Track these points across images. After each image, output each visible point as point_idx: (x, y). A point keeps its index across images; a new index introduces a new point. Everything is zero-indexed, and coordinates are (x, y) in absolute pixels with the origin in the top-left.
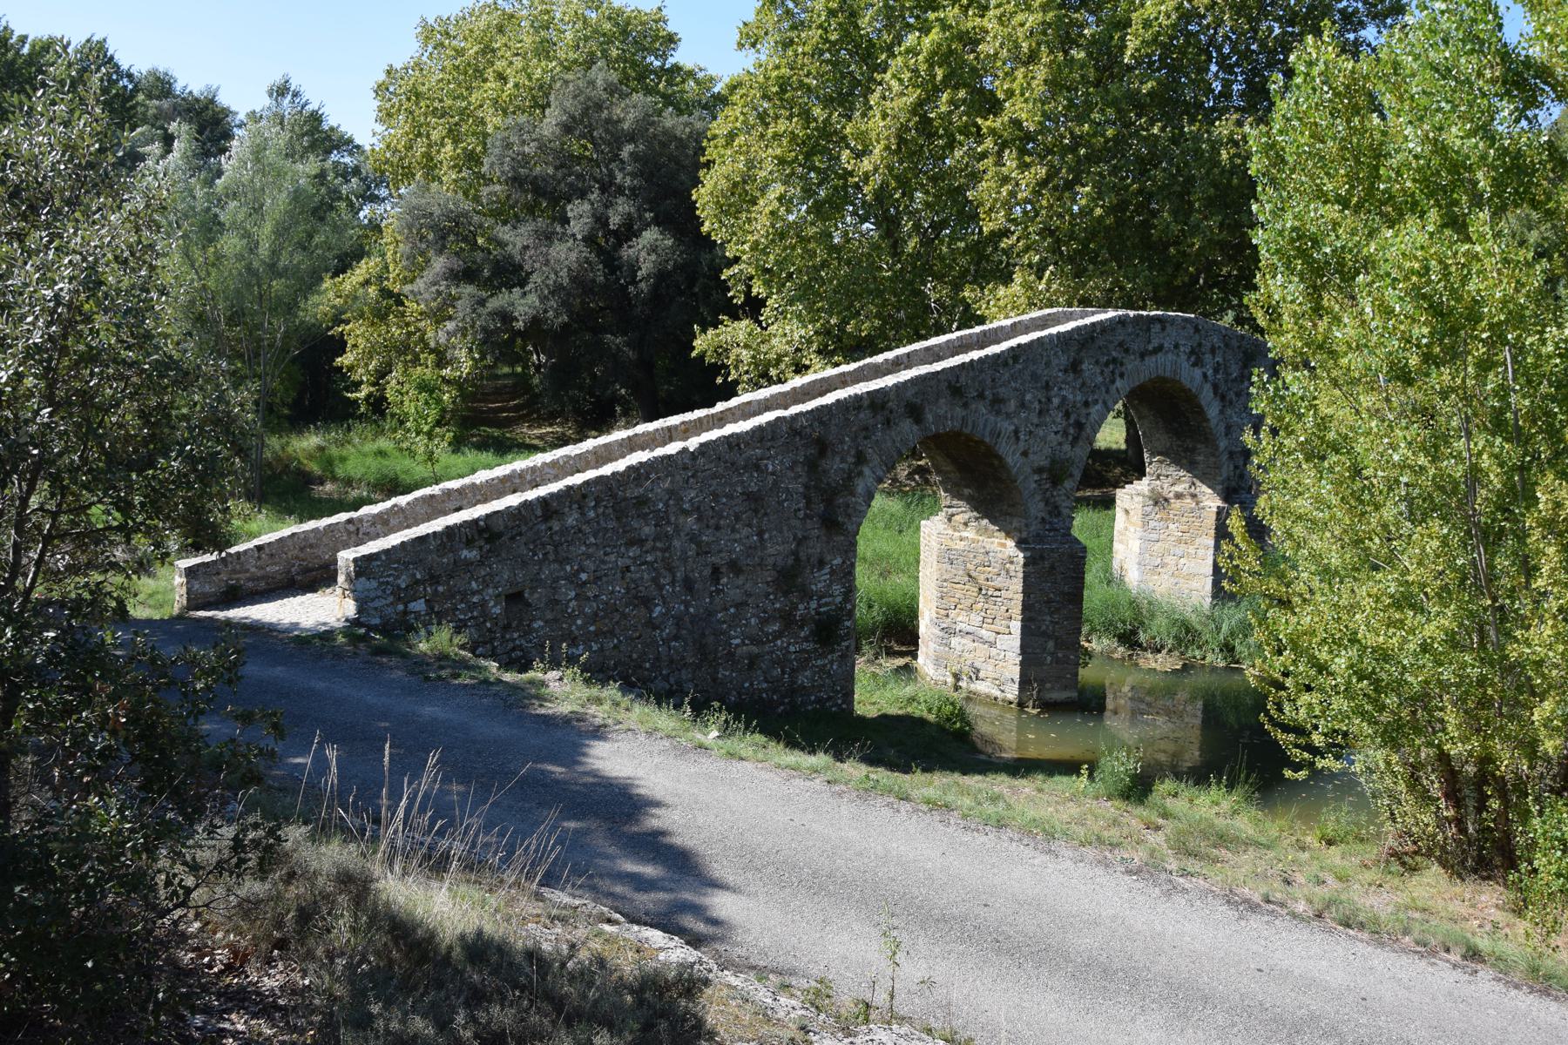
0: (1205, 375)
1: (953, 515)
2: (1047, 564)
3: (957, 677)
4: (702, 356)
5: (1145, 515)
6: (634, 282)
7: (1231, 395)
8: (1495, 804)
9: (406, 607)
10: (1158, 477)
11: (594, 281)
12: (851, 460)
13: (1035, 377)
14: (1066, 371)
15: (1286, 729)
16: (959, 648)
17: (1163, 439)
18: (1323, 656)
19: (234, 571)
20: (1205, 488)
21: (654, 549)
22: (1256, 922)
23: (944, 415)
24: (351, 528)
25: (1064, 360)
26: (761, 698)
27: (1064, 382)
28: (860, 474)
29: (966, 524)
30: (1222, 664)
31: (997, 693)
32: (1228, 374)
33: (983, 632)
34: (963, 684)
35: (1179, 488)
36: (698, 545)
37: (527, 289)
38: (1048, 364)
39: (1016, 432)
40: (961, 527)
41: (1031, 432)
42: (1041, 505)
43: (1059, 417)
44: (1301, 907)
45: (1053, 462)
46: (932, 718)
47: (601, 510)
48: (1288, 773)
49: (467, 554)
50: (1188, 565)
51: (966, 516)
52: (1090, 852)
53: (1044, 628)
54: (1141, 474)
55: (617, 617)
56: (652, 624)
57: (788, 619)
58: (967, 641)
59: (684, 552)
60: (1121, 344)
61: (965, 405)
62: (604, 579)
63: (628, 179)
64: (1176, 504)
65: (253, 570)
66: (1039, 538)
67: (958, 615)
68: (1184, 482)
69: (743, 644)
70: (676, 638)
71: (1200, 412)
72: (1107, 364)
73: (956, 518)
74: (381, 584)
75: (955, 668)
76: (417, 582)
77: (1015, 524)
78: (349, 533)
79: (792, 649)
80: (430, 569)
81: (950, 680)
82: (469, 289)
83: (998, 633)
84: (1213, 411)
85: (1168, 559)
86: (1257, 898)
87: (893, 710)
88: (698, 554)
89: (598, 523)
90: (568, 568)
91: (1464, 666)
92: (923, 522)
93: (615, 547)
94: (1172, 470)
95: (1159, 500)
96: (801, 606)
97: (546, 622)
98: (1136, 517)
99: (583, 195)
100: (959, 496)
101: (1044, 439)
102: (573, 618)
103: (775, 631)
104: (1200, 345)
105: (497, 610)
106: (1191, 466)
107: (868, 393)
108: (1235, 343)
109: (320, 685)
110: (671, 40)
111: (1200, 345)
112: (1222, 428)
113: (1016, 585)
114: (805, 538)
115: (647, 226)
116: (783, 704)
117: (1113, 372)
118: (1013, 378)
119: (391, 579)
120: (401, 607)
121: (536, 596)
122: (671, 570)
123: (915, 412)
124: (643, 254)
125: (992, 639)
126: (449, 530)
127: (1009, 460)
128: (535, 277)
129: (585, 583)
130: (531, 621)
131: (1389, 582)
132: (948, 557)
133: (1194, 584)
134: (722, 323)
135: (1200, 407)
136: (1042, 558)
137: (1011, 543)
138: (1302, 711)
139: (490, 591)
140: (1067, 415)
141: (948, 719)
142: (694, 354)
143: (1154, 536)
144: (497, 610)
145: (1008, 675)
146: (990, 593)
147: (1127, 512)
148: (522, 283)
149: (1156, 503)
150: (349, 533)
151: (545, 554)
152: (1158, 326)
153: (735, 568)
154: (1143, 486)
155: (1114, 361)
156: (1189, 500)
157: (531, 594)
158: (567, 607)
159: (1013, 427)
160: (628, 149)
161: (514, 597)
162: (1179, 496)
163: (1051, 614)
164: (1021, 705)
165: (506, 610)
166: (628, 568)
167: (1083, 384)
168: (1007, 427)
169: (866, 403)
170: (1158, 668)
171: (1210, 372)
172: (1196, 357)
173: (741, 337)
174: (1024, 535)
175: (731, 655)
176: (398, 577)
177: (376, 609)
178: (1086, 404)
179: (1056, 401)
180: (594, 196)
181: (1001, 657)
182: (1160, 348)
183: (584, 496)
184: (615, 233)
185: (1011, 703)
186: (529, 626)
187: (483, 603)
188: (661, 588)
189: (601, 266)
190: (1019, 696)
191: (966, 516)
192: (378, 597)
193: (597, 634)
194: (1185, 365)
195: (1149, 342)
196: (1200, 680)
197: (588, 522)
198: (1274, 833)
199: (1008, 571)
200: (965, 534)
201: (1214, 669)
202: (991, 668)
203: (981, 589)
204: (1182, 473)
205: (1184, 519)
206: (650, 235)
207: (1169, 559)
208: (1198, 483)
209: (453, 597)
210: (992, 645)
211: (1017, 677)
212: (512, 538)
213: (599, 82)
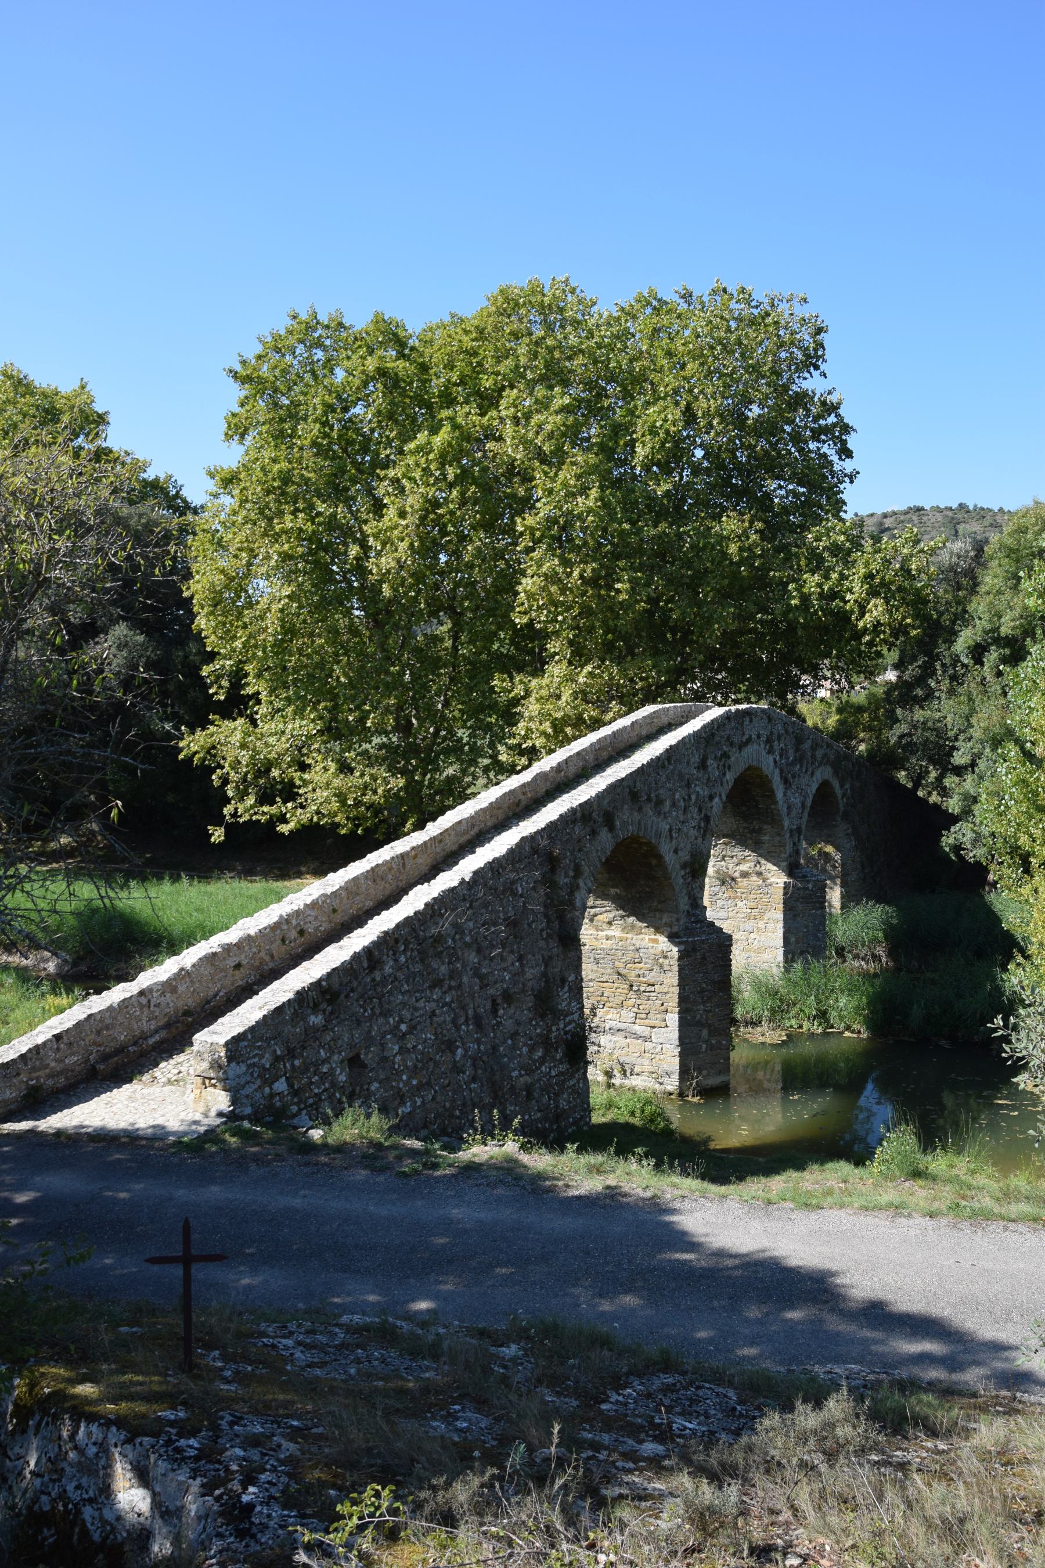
0: (775, 762)
1: (596, 915)
2: (699, 955)
4: (189, 759)
9: (271, 1089)
10: (724, 857)
12: (571, 874)
13: (681, 776)
14: (698, 768)
16: (610, 1046)
19: (34, 1069)
20: (770, 866)
21: (450, 988)
25: (696, 759)
26: (537, 1127)
28: (578, 887)
29: (610, 923)
30: (820, 1031)
33: (637, 1028)
34: (617, 1081)
35: (744, 867)
36: (481, 977)
38: (688, 763)
39: (670, 830)
40: (605, 926)
41: (679, 830)
42: (686, 898)
46: (637, 1121)
47: (409, 954)
50: (758, 939)
51: (611, 915)
53: (698, 1017)
55: (431, 1065)
56: (457, 1069)
57: (546, 1042)
58: (618, 1038)
59: (471, 987)
61: (640, 809)
62: (419, 1027)
64: (743, 882)
65: (53, 1064)
66: (689, 931)
67: (607, 1013)
68: (748, 861)
69: (521, 1075)
70: (474, 1079)
71: (771, 795)
73: (599, 917)
74: (249, 1066)
75: (607, 1066)
77: (665, 919)
78: (142, 1006)
79: (553, 1073)
80: (287, 1043)
83: (654, 1027)
84: (779, 795)
88: (481, 988)
89: (407, 967)
90: (391, 1020)
93: (422, 991)
94: (738, 852)
96: (554, 1028)
97: (380, 1083)
100: (604, 896)
102: (399, 1073)
103: (540, 1058)
107: (580, 805)
109: (297, 1202)
112: (785, 809)
113: (671, 981)
114: (551, 958)
115: (114, 621)
116: (552, 1131)
117: (724, 765)
119: (256, 1060)
120: (267, 1090)
121: (370, 1055)
122: (464, 1008)
125: (647, 1034)
126: (301, 995)
127: (667, 859)
129: (404, 1035)
130: (369, 1084)
134: (212, 723)
136: (694, 950)
137: (663, 939)
139: (336, 1057)
140: (700, 810)
141: (652, 1121)
142: (181, 757)
144: (343, 1078)
145: (666, 1067)
146: (642, 989)
149: (723, 883)
150: (142, 1006)
151: (372, 1009)
152: (748, 719)
153: (508, 997)
156: (755, 878)
157: (366, 1054)
158: (394, 1063)
159: (668, 827)
161: (354, 1062)
162: (745, 875)
163: (704, 1003)
164: (681, 1095)
165: (350, 1076)
166: (433, 1014)
167: (708, 779)
169: (579, 814)
170: (768, 1041)
171: (778, 758)
173: (238, 736)
174: (675, 929)
175: (513, 1087)
176: (262, 1057)
177: (247, 1096)
178: (711, 798)
181: (658, 1049)
182: (749, 740)
185: (671, 1094)
186: (368, 1089)
188: (458, 1028)
191: (611, 915)
192: (248, 1083)
193: (420, 1087)
194: (764, 753)
195: (744, 734)
197: (400, 969)
199: (661, 966)
200: (610, 933)
201: (812, 1035)
202: (646, 1062)
203: (631, 986)
204: (746, 853)
205: (752, 896)
206: (121, 630)
208: (763, 862)
209: (307, 1070)
210: (647, 1039)
212: (347, 996)
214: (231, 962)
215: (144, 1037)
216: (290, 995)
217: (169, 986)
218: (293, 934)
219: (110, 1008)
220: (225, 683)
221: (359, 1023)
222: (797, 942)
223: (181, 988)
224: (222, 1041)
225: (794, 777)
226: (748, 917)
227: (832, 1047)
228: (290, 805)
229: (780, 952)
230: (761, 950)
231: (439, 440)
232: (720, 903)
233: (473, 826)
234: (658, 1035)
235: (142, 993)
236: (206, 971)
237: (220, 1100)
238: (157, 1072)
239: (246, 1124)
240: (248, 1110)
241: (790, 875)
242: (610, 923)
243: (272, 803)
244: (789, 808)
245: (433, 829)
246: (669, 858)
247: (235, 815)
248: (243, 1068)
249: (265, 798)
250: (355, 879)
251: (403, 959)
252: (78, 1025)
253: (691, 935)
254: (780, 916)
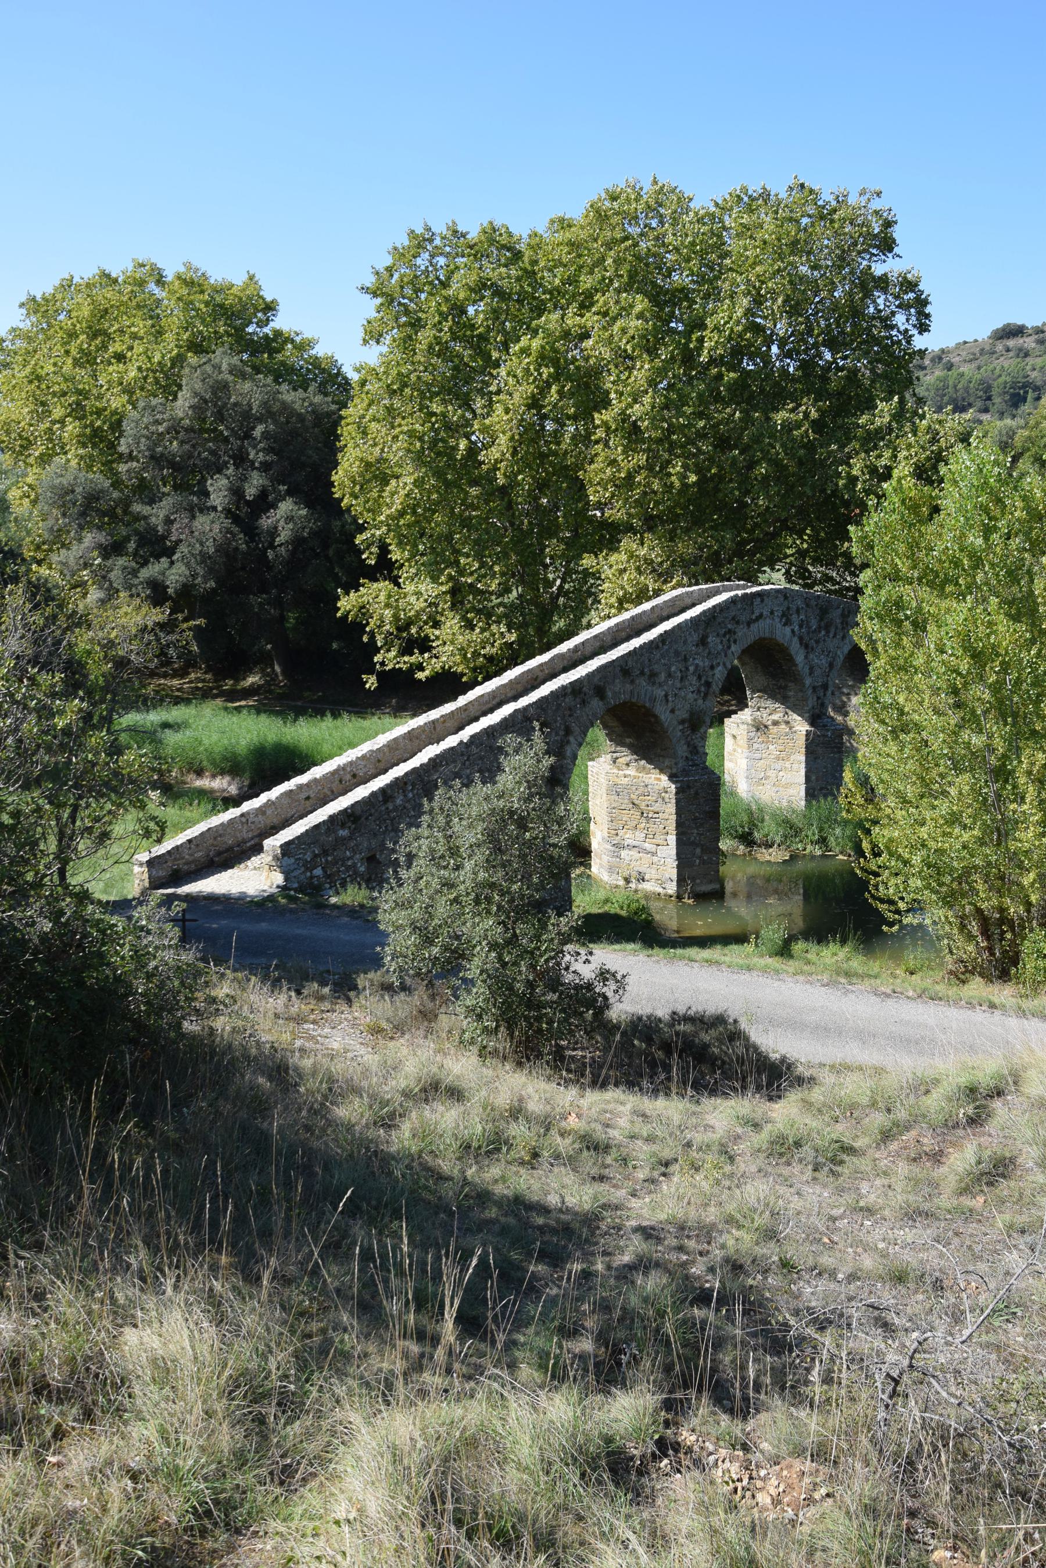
0: (793, 631)
2: (692, 791)
3: (627, 880)
4: (345, 616)
5: (750, 739)
6: (272, 546)
7: (812, 643)
8: (1009, 936)
11: (237, 549)
12: (562, 733)
13: (677, 653)
15: (882, 901)
16: (628, 858)
17: (761, 680)
18: (907, 856)
20: (795, 716)
22: (890, 1002)
23: (619, 691)
24: (244, 820)
25: (695, 637)
27: (697, 654)
28: (568, 742)
29: (628, 765)
30: (819, 853)
31: (660, 890)
32: (809, 627)
33: (647, 846)
34: (633, 885)
35: (775, 717)
37: (175, 558)
38: (685, 642)
39: (666, 696)
43: (694, 680)
44: (911, 993)
45: (692, 714)
46: (624, 913)
48: (885, 928)
49: (343, 833)
50: (786, 777)
51: (628, 759)
52: (801, 978)
54: (742, 705)
58: (634, 853)
60: (733, 619)
61: (632, 682)
63: (261, 454)
64: (774, 730)
66: (685, 772)
71: (790, 660)
72: (724, 635)
75: (626, 874)
76: (316, 856)
81: (621, 883)
82: (121, 561)
84: (800, 658)
85: (769, 773)
86: (889, 991)
87: (595, 910)
91: (987, 856)
92: (590, 763)
94: (769, 703)
95: (759, 727)
98: (742, 741)
99: (219, 471)
101: (684, 698)
104: (788, 608)
105: (362, 869)
106: (784, 700)
108: (813, 603)
110: (270, 308)
111: (788, 608)
112: (807, 670)
113: (671, 809)
118: (663, 656)
123: (600, 692)
124: (282, 523)
126: (332, 818)
127: (663, 717)
128: (183, 549)
131: (944, 807)
132: (615, 790)
133: (792, 791)
135: (790, 655)
136: (689, 787)
137: (664, 778)
138: (891, 891)
140: (700, 677)
141: (636, 913)
142: (339, 615)
143: (758, 755)
144: (362, 869)
147: (734, 737)
148: (169, 552)
149: (758, 730)
154: (746, 715)
155: (730, 631)
156: (783, 726)
160: (259, 430)
162: (776, 723)
163: (697, 828)
164: (679, 897)
165: (368, 868)
168: (660, 693)
171: (796, 628)
172: (786, 618)
173: (382, 598)
174: (674, 771)
178: (712, 668)
179: (692, 668)
180: (231, 471)
183: (406, 783)
184: (248, 503)
187: (354, 865)
189: (242, 536)
190: (678, 891)
191: (628, 759)
194: (779, 625)
196: (800, 866)
197: (409, 801)
198: (876, 969)
200: (627, 772)
201: (813, 857)
207: (771, 773)
210: (654, 854)
211: (675, 877)
213: (225, 367)
214: (303, 796)
215: (244, 842)
216: (325, 818)
217: (261, 811)
218: (348, 777)
219: (222, 824)
220: (374, 549)
221: (375, 835)
222: (817, 780)
223: (269, 812)
224: (278, 844)
225: (817, 642)
226: (778, 758)
227: (829, 866)
228: (426, 655)
229: (803, 788)
230: (788, 785)
231: (536, 344)
232: (756, 746)
233: (494, 697)
234: (663, 851)
235: (242, 815)
236: (285, 801)
237: (279, 878)
238: (249, 863)
239: (292, 893)
240: (296, 885)
241: (812, 724)
242: (628, 765)
243: (411, 654)
244: (812, 670)
245: (462, 701)
247: (383, 664)
248: (293, 860)
249: (406, 651)
250: (395, 740)
251: (410, 795)
252: (202, 834)
254: (803, 758)
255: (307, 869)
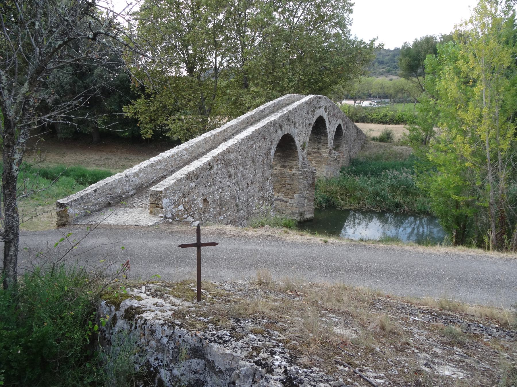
61: (290, 125)
65: (93, 201)
74: (170, 200)
78: (127, 181)
136: (304, 173)
144: (201, 206)
161: (205, 200)
162: (314, 153)
165: (204, 205)
175: (253, 213)
176: (175, 196)
187: (198, 204)
197: (219, 169)
210: (287, 202)
246: (297, 143)
248: (168, 200)
253: (303, 168)
255: (176, 205)
